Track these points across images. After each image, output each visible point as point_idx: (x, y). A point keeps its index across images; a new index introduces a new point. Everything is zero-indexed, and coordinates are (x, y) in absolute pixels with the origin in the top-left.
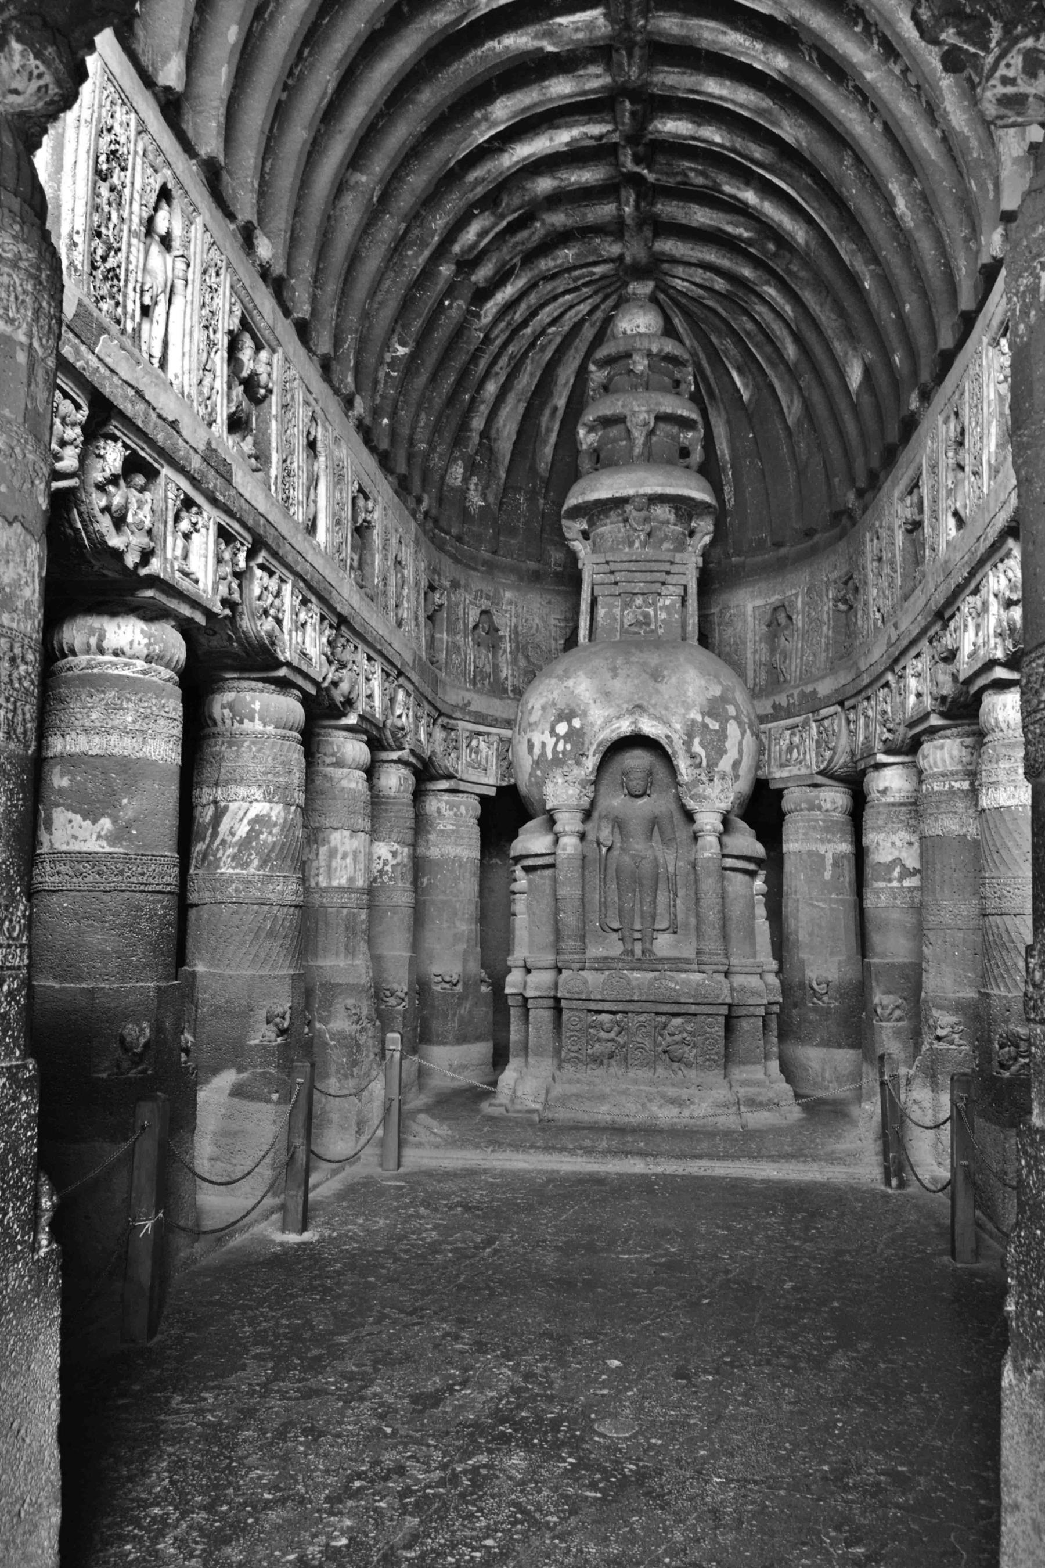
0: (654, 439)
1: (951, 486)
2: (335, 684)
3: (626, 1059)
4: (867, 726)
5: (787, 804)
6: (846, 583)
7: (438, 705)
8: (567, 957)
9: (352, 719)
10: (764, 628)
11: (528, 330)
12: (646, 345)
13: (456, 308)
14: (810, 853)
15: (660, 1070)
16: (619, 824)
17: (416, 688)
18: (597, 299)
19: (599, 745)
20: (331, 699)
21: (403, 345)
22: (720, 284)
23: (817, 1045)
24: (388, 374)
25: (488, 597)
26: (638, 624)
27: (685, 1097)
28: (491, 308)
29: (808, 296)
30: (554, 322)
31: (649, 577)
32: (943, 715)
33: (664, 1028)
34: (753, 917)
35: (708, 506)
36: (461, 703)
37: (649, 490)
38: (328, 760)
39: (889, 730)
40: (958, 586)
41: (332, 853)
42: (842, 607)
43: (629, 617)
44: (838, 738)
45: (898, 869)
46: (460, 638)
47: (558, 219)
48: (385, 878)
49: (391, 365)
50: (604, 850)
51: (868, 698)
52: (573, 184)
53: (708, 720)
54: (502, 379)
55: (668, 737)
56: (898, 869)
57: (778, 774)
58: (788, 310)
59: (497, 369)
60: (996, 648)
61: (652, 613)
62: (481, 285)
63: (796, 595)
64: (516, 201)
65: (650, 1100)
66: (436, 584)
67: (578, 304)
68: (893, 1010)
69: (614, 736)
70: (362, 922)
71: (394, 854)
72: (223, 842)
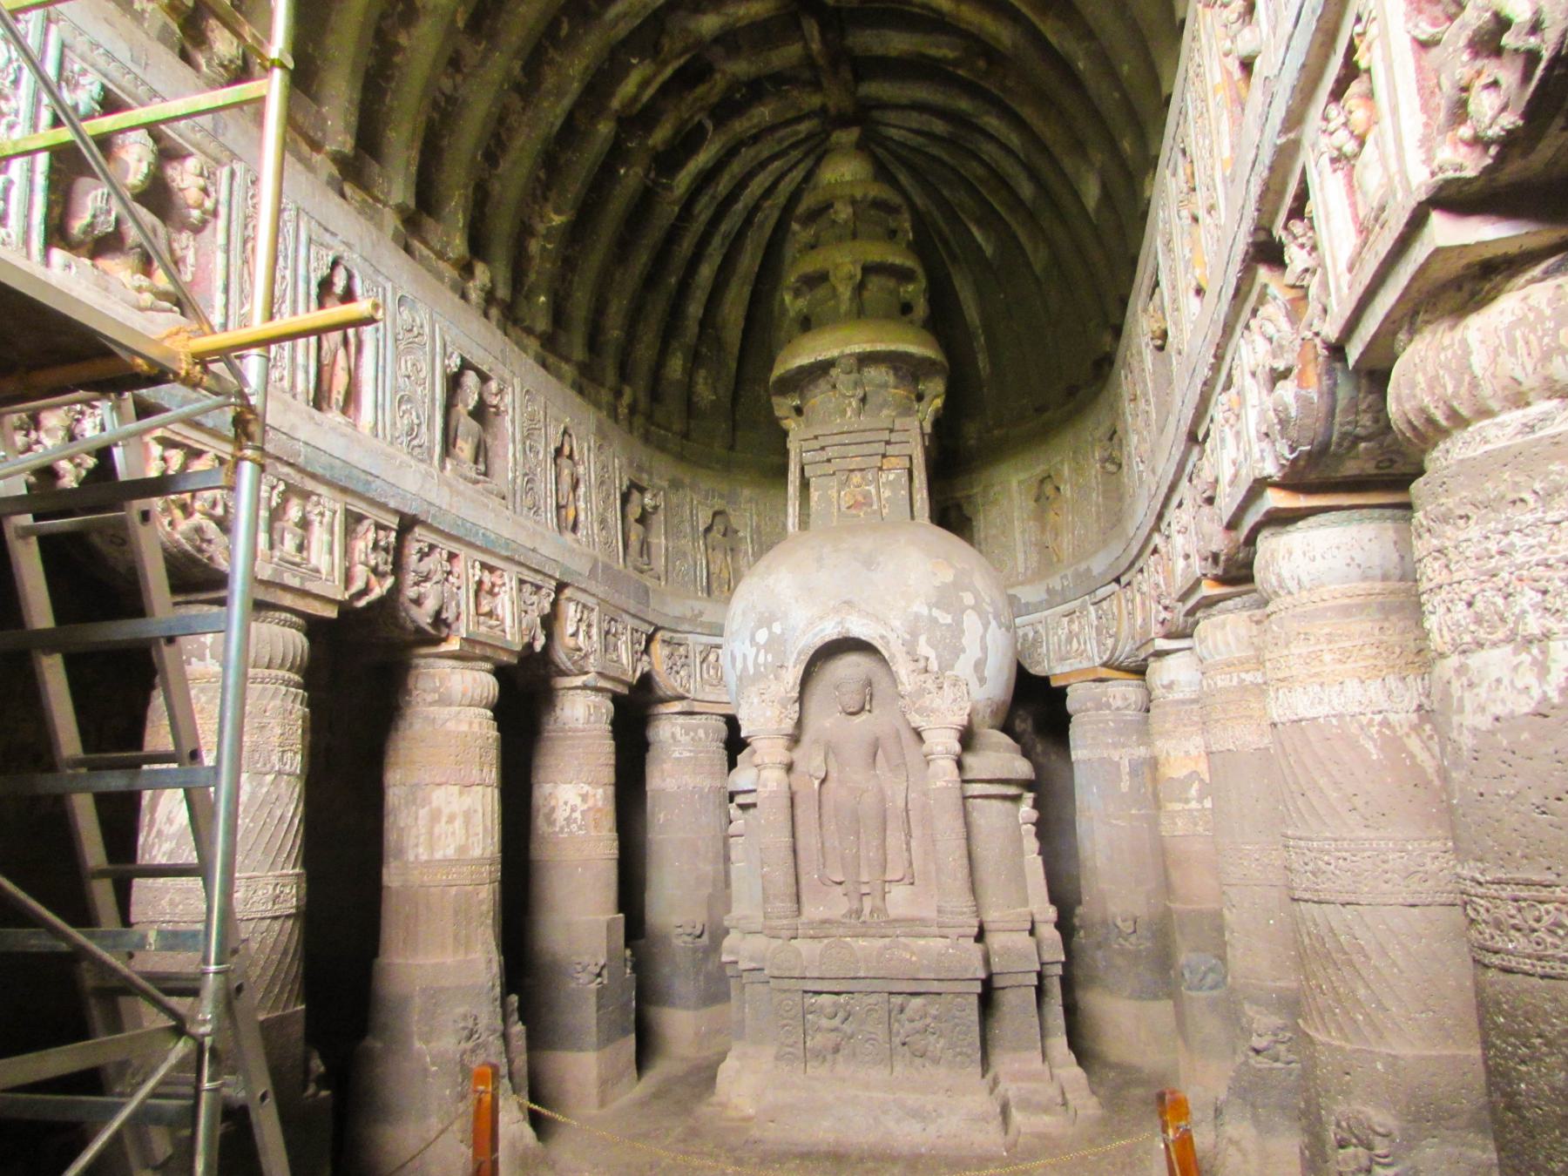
0: (866, 294)
1: (1188, 255)
2: (418, 602)
3: (854, 1055)
4: (1143, 604)
5: (1071, 705)
6: (1111, 439)
7: (650, 618)
8: (774, 923)
9: (453, 645)
10: (1032, 504)
11: (739, 206)
12: (847, 191)
13: (631, 176)
14: (1102, 760)
15: (898, 1069)
16: (830, 750)
17: (602, 602)
18: (809, 162)
19: (799, 654)
20: (413, 621)
21: (558, 211)
22: (939, 127)
23: (1129, 998)
24: (544, 248)
25: (721, 496)
26: (856, 505)
27: (929, 1107)
28: (683, 179)
29: (1027, 112)
30: (769, 192)
31: (866, 449)
32: (1221, 580)
33: (902, 1011)
34: (1020, 852)
35: (932, 363)
36: (689, 614)
37: (857, 349)
38: (430, 697)
39: (1166, 608)
40: (1205, 384)
41: (435, 817)
42: (1111, 467)
43: (847, 499)
44: (1119, 623)
45: (1196, 785)
46: (686, 543)
47: (741, 68)
48: (574, 827)
49: (547, 237)
50: (817, 783)
51: (1141, 571)
52: (739, 19)
53: (936, 613)
54: (717, 260)
55: (882, 637)
56: (1196, 785)
57: (1058, 670)
58: (1014, 140)
59: (710, 250)
60: (1263, 459)
61: (873, 491)
62: (661, 148)
63: (1062, 462)
64: (679, 45)
65: (885, 1112)
66: (645, 484)
67: (790, 169)
68: (1205, 974)
69: (818, 642)
70: (481, 902)
71: (584, 797)
72: (160, 833)
